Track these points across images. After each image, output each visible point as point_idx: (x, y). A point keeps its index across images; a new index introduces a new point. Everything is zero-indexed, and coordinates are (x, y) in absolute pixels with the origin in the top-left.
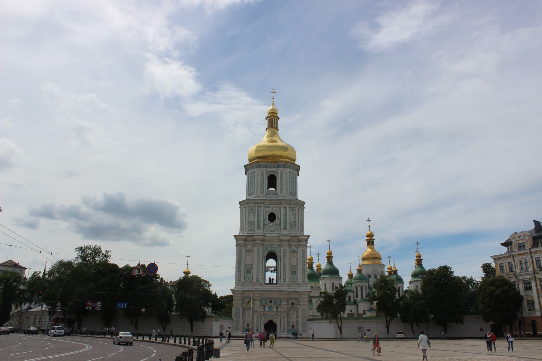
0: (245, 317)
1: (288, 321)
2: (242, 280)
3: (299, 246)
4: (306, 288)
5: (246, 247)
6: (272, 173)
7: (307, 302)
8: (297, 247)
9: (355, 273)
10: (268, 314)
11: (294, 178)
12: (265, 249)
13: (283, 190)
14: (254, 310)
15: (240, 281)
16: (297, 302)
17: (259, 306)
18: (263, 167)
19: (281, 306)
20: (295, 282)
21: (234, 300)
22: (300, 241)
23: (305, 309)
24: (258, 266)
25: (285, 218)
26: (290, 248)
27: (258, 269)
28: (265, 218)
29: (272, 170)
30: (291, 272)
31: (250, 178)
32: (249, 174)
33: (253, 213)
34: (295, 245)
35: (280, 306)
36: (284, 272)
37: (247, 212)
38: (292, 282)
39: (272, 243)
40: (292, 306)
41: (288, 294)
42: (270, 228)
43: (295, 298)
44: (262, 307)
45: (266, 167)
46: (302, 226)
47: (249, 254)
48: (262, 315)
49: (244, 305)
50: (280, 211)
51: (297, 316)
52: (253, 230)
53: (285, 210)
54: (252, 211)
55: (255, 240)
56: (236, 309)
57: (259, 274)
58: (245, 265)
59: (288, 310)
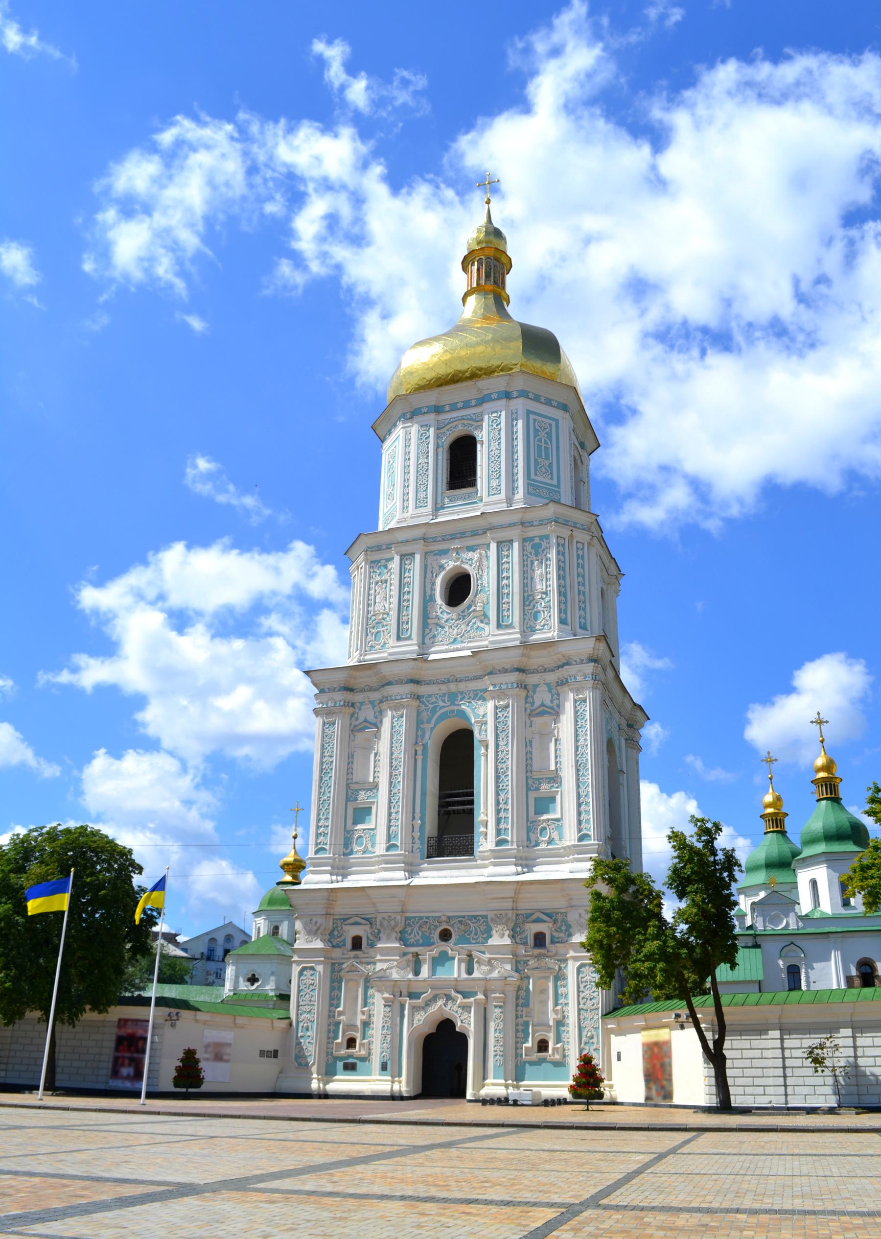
6: (460, 428)
8: (558, 694)
11: (549, 435)
12: (425, 714)
16: (561, 931)
18: (425, 413)
22: (568, 664)
25: (505, 582)
28: (428, 593)
33: (386, 581)
34: (548, 685)
36: (498, 803)
40: (537, 951)
45: (438, 410)
46: (584, 610)
56: (301, 973)
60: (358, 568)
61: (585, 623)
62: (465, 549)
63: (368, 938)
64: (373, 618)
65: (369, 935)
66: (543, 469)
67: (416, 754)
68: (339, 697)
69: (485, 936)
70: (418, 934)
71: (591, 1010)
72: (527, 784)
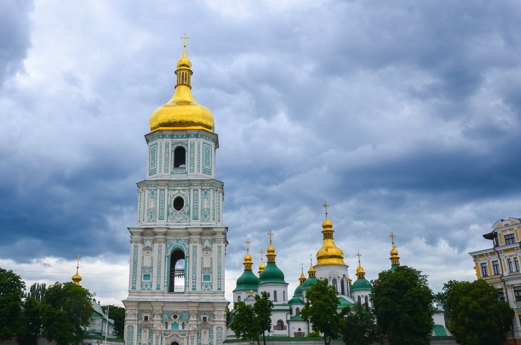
0: (140, 338)
1: (198, 343)
2: (138, 288)
3: (213, 241)
4: (222, 298)
5: (143, 243)
6: (180, 145)
7: (223, 317)
8: (212, 244)
9: (307, 276)
10: (171, 334)
11: (209, 151)
12: (168, 246)
13: (194, 166)
14: (153, 329)
15: (135, 289)
17: (160, 322)
18: (167, 138)
19: (190, 323)
20: (209, 290)
21: (127, 315)
22: (216, 234)
23: (221, 327)
24: (159, 268)
25: (196, 204)
26: (202, 243)
27: (159, 273)
29: (180, 141)
30: (203, 277)
31: (152, 151)
32: (150, 146)
34: (209, 240)
35: (188, 323)
36: (193, 277)
37: (147, 196)
38: (204, 290)
39: (178, 238)
41: (198, 307)
42: (175, 217)
43: (208, 312)
44: (164, 325)
45: (172, 137)
46: (219, 215)
47: (148, 252)
48: (163, 334)
49: (140, 322)
50: (190, 195)
51: (211, 337)
52: (153, 221)
53: (196, 194)
54: (152, 195)
55: (155, 234)
57: (160, 280)
58: (142, 267)
59: (198, 328)
60: (143, 190)
61: (219, 220)
62: (182, 190)
63: (150, 317)
64: (150, 210)
65: (150, 316)
66: (207, 164)
67: (165, 259)
68: (139, 237)
69: (188, 317)
70: (167, 316)
71: (220, 340)
72: (201, 271)
